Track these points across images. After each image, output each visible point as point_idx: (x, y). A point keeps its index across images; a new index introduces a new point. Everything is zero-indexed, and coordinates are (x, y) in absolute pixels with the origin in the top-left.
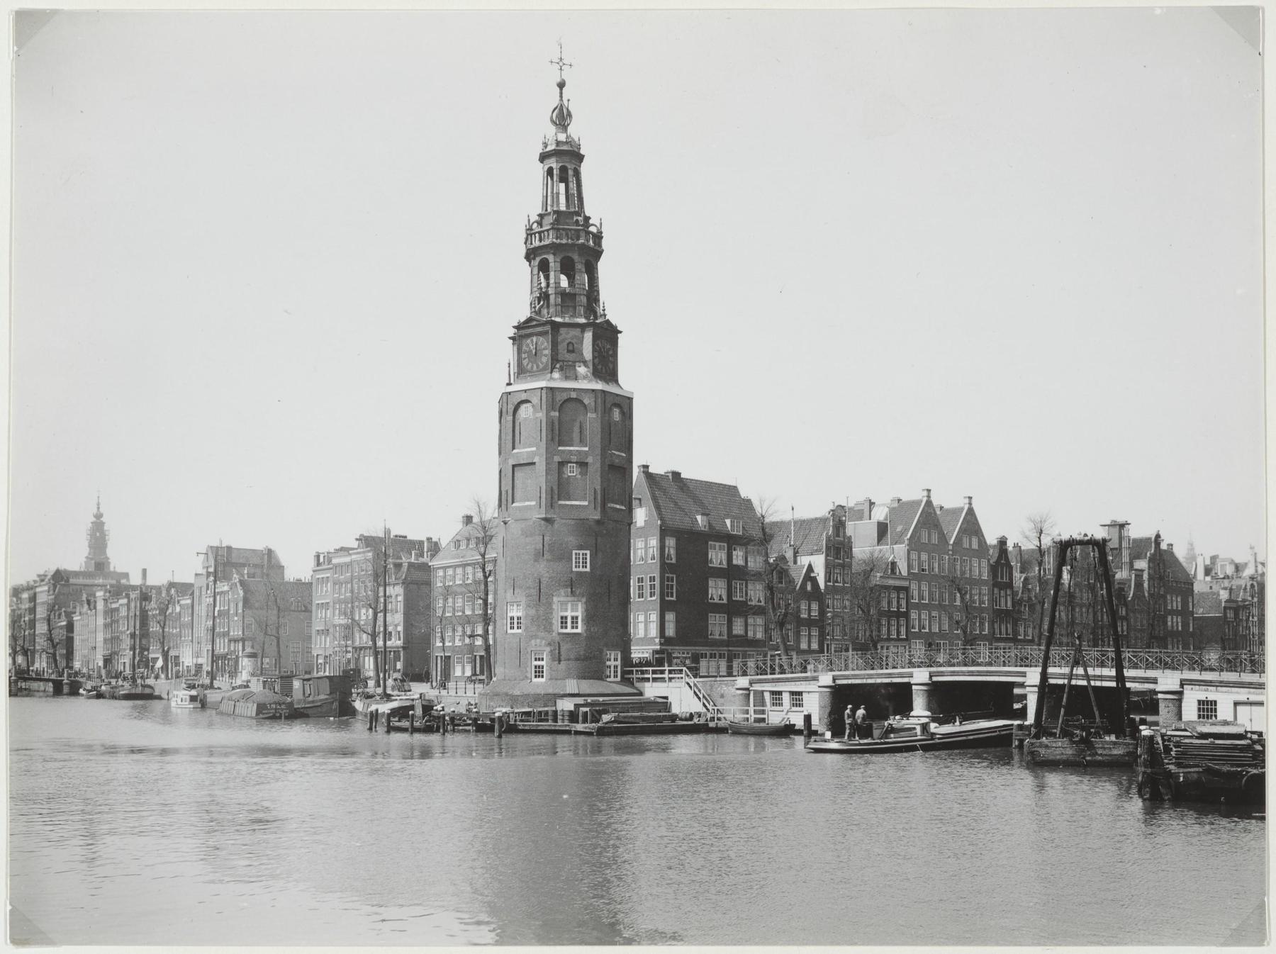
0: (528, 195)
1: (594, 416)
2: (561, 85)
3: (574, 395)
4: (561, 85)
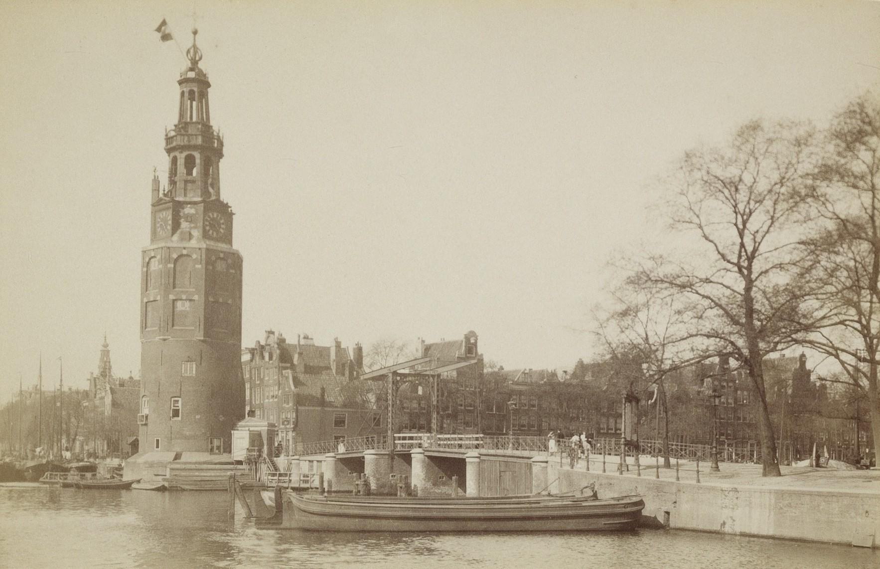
1: (200, 266)
2: (195, 33)
3: (185, 252)
4: (195, 33)
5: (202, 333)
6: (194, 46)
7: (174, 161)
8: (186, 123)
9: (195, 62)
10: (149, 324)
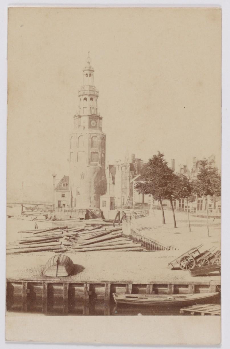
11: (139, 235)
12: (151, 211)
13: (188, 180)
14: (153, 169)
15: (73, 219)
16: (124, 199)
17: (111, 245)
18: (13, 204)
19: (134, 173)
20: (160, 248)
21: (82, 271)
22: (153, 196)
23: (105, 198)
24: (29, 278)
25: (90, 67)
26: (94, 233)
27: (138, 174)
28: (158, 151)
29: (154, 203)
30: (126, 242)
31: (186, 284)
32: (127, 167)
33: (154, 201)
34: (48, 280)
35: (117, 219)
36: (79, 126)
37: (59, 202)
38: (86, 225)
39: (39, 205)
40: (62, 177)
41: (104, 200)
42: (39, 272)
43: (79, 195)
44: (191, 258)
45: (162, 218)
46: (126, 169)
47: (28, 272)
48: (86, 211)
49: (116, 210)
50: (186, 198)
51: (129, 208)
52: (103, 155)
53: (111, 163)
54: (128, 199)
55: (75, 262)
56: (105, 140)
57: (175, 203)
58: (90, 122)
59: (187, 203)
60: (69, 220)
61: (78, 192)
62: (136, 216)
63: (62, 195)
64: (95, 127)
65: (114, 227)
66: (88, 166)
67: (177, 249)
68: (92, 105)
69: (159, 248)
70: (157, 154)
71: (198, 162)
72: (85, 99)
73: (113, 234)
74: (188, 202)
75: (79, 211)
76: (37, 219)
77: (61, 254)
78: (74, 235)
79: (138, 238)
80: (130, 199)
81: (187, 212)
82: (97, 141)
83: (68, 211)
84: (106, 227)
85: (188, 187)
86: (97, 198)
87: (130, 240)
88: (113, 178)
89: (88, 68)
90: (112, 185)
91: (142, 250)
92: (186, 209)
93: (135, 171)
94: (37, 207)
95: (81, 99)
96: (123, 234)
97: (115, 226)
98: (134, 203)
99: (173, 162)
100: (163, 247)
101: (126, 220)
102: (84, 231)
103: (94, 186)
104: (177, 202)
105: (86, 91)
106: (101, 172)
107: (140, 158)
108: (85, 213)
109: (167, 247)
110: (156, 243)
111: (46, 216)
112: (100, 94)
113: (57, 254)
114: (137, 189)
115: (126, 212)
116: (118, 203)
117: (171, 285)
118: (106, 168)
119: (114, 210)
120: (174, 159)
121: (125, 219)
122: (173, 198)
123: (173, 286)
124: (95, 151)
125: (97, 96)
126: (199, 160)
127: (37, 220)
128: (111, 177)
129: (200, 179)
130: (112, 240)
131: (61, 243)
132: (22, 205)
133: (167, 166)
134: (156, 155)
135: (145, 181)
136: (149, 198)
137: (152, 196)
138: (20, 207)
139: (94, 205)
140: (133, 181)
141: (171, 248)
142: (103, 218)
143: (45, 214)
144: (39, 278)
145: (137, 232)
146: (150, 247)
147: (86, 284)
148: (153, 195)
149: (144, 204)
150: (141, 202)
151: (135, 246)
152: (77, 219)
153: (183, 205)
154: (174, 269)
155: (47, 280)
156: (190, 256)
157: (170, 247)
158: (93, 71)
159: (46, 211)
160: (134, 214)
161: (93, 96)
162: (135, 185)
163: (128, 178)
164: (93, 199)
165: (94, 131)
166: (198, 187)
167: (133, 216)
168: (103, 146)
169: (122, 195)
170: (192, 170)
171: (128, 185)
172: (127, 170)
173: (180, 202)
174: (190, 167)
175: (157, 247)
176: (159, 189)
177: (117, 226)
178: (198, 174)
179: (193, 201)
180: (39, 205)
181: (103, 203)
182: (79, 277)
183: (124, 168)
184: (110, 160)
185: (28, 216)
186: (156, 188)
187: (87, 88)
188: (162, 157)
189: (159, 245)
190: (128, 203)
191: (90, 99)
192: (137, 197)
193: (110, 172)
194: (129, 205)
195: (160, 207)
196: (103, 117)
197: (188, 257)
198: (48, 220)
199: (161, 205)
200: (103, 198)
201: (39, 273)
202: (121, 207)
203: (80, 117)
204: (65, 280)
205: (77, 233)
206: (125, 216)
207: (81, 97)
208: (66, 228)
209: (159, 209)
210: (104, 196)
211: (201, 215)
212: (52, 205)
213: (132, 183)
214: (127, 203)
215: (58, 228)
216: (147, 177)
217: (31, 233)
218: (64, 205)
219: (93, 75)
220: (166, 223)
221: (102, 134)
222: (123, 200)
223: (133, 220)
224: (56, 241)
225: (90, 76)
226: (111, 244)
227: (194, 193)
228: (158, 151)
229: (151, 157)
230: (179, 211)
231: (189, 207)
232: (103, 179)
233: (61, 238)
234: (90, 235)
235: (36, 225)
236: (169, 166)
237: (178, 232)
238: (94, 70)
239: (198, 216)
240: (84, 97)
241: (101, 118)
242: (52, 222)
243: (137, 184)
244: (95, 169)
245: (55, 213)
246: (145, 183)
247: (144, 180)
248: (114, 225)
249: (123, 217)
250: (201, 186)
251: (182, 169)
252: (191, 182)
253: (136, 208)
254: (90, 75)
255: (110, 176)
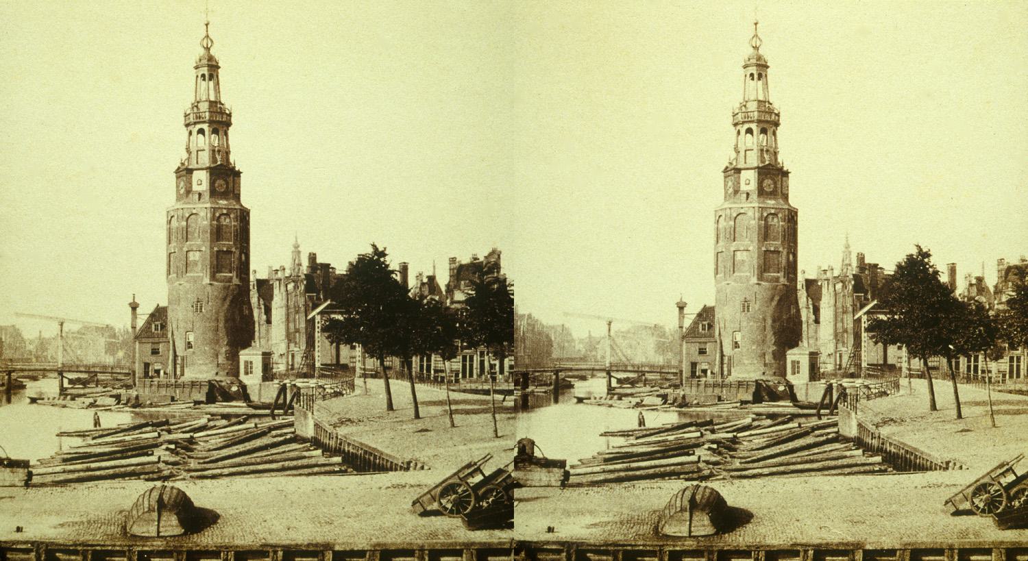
0: (186, 90)
1: (205, 222)
4: (207, 25)
5: (208, 277)
6: (207, 36)
7: (190, 133)
8: (198, 102)
9: (208, 49)
10: (171, 270)
11: (877, 435)
12: (903, 382)
13: (988, 310)
14: (906, 288)
15: (725, 402)
16: (841, 356)
17: (812, 461)
18: (587, 372)
19: (863, 298)
20: (925, 466)
21: (748, 522)
22: (908, 349)
23: (798, 355)
24: (625, 540)
25: (759, 58)
26: (772, 434)
27: (873, 300)
28: (917, 246)
29: (909, 363)
30: (848, 453)
31: (987, 547)
32: (847, 283)
33: (909, 358)
34: (669, 543)
35: (827, 401)
36: (736, 192)
37: (694, 365)
38: (754, 416)
39: (648, 372)
40: (698, 309)
41: (795, 358)
42: (649, 526)
43: (737, 349)
44: (996, 487)
45: (928, 397)
46: (844, 287)
47: (624, 527)
48: (754, 384)
49: (823, 381)
50: (983, 352)
51: (852, 376)
52: (791, 257)
53: (812, 276)
54: (850, 357)
55: (731, 501)
56: (796, 223)
57: (957, 364)
58: (760, 183)
59: (984, 363)
60: (716, 404)
61: (736, 343)
62: (870, 393)
63: (700, 349)
64: (773, 194)
65: (820, 419)
66: (758, 284)
67: (964, 467)
68: (765, 144)
69: (923, 465)
70: (914, 251)
71: (1009, 269)
72: (749, 131)
73: (818, 436)
74: (988, 359)
75: (739, 385)
76: (643, 403)
77: (700, 484)
78: (727, 439)
79: (875, 442)
80: (856, 355)
81: (986, 383)
82: (778, 223)
83: (715, 385)
84: (803, 420)
85: (987, 326)
86: (780, 356)
87: (856, 449)
88: (816, 310)
89: (754, 61)
90: (813, 326)
91: (885, 471)
92: (984, 375)
93: (866, 293)
94: (644, 378)
95: (739, 132)
96: (841, 435)
97: (822, 417)
98: (864, 365)
99: (953, 271)
100: (931, 462)
101: (846, 403)
102: (751, 429)
103: (773, 327)
104: (963, 361)
105: (752, 113)
106: (786, 298)
107: (876, 263)
108: (753, 389)
109: (942, 463)
110: (917, 453)
111: (664, 397)
112: (783, 120)
113: (689, 483)
114: (871, 334)
115: (845, 385)
116: (827, 366)
117: (951, 549)
118: (799, 287)
119: (819, 380)
120: (953, 264)
121: (845, 401)
122: (954, 351)
123: (956, 551)
124: (772, 249)
125: (777, 124)
126: (1011, 264)
127: (644, 406)
128: (811, 306)
129: (1012, 309)
130: (816, 450)
131: (699, 457)
132: (609, 373)
133: (939, 279)
134: (912, 255)
135: (888, 316)
136: (897, 354)
137: (904, 349)
138: (604, 378)
139: (774, 371)
140: (861, 316)
141: (951, 464)
142: (792, 397)
143: (662, 392)
144: (649, 541)
145: (872, 428)
146: (902, 462)
147: (756, 552)
148: (908, 346)
149: (885, 368)
150: (881, 362)
151: (868, 462)
152: (735, 403)
153: (976, 367)
154: (958, 513)
155: (667, 545)
156: (993, 483)
157: (948, 463)
158: (768, 67)
159: (665, 386)
160: (865, 390)
161: (768, 122)
162: (864, 325)
163: (851, 309)
164: (769, 358)
165: (771, 202)
166: (1010, 326)
167: (861, 394)
168: (791, 236)
169: (836, 348)
170: (996, 287)
171: (850, 325)
172: (846, 291)
173: (969, 361)
174: (991, 281)
175: (920, 463)
176: (920, 331)
177: (826, 417)
178: (1009, 297)
179: (997, 357)
180: (646, 374)
181: (793, 367)
182: (740, 536)
183: (839, 286)
184: (807, 268)
185: (623, 398)
186: (914, 329)
187: (753, 106)
188: (926, 260)
189: (923, 459)
190: (851, 365)
191: (759, 132)
192: (871, 353)
193: (808, 296)
194: (852, 370)
195: (923, 372)
196: (789, 171)
197: (990, 485)
198: (669, 407)
199: (926, 369)
200: (792, 355)
201: (646, 529)
202: (835, 375)
203: (738, 171)
204: (710, 545)
205: (735, 434)
206: (843, 395)
207: (739, 127)
208: (711, 423)
209: (921, 376)
210: (795, 350)
211: (1017, 388)
212: (676, 373)
213: (859, 320)
214: (848, 366)
215: (690, 425)
216: (893, 306)
217: (631, 438)
218: (705, 371)
219: (766, 76)
220: (938, 408)
221: (788, 209)
222: (838, 358)
223: (863, 401)
224: (688, 454)
225: (759, 79)
226: (812, 458)
227: (1000, 341)
228: (917, 246)
229: (901, 258)
230: (968, 380)
231: (990, 372)
232: (793, 311)
233: (698, 446)
234: (764, 438)
235: (641, 417)
236: (944, 278)
237: (966, 428)
238: (768, 64)
239: (1010, 392)
240: (746, 126)
241: (786, 174)
242: (676, 411)
243: (869, 322)
244: (775, 288)
245: (683, 390)
246: (889, 318)
247: (885, 314)
248: (820, 416)
249: (839, 395)
250: (1015, 324)
251: (971, 285)
252: (993, 316)
253: (870, 376)
254: (760, 76)
255: (808, 305)
